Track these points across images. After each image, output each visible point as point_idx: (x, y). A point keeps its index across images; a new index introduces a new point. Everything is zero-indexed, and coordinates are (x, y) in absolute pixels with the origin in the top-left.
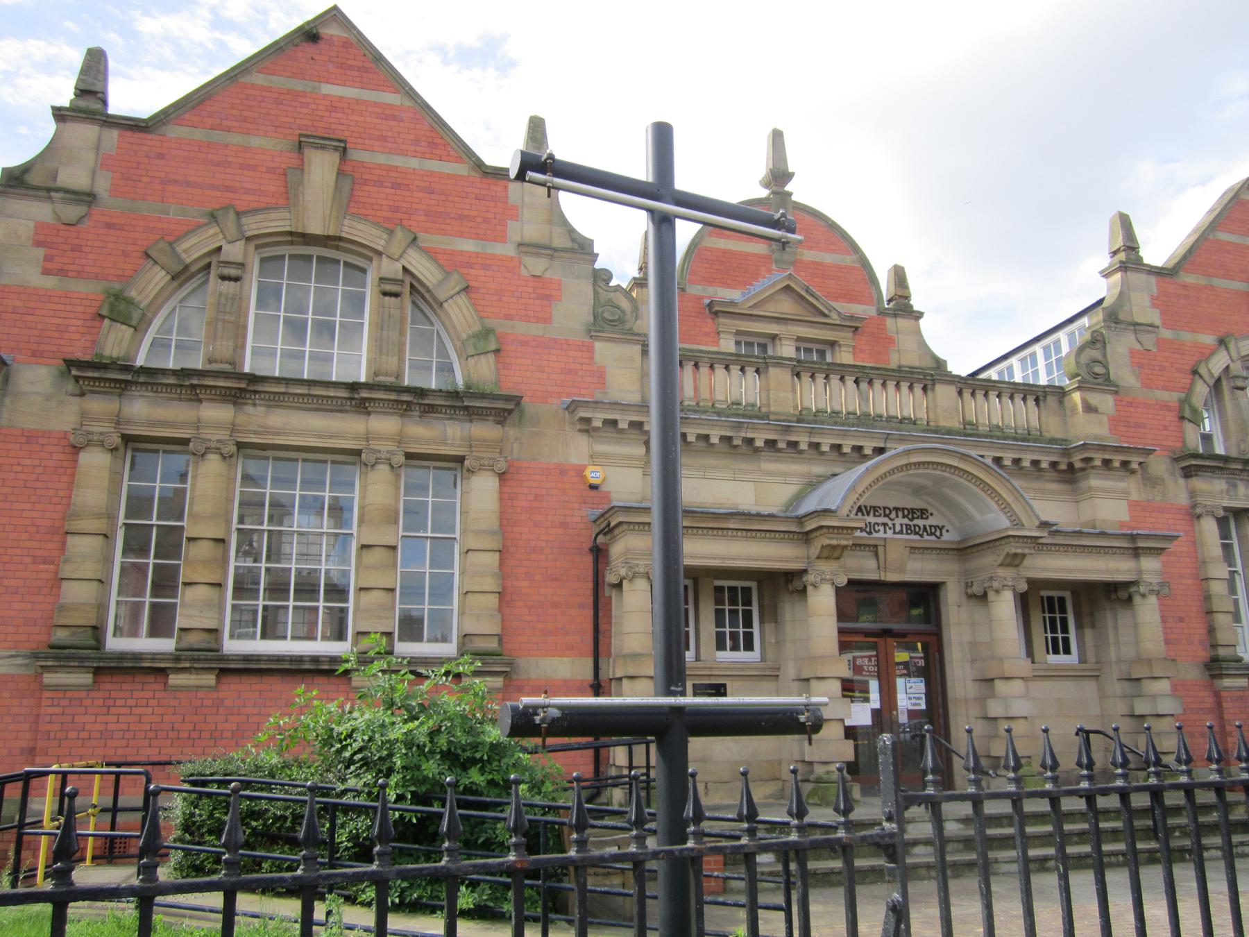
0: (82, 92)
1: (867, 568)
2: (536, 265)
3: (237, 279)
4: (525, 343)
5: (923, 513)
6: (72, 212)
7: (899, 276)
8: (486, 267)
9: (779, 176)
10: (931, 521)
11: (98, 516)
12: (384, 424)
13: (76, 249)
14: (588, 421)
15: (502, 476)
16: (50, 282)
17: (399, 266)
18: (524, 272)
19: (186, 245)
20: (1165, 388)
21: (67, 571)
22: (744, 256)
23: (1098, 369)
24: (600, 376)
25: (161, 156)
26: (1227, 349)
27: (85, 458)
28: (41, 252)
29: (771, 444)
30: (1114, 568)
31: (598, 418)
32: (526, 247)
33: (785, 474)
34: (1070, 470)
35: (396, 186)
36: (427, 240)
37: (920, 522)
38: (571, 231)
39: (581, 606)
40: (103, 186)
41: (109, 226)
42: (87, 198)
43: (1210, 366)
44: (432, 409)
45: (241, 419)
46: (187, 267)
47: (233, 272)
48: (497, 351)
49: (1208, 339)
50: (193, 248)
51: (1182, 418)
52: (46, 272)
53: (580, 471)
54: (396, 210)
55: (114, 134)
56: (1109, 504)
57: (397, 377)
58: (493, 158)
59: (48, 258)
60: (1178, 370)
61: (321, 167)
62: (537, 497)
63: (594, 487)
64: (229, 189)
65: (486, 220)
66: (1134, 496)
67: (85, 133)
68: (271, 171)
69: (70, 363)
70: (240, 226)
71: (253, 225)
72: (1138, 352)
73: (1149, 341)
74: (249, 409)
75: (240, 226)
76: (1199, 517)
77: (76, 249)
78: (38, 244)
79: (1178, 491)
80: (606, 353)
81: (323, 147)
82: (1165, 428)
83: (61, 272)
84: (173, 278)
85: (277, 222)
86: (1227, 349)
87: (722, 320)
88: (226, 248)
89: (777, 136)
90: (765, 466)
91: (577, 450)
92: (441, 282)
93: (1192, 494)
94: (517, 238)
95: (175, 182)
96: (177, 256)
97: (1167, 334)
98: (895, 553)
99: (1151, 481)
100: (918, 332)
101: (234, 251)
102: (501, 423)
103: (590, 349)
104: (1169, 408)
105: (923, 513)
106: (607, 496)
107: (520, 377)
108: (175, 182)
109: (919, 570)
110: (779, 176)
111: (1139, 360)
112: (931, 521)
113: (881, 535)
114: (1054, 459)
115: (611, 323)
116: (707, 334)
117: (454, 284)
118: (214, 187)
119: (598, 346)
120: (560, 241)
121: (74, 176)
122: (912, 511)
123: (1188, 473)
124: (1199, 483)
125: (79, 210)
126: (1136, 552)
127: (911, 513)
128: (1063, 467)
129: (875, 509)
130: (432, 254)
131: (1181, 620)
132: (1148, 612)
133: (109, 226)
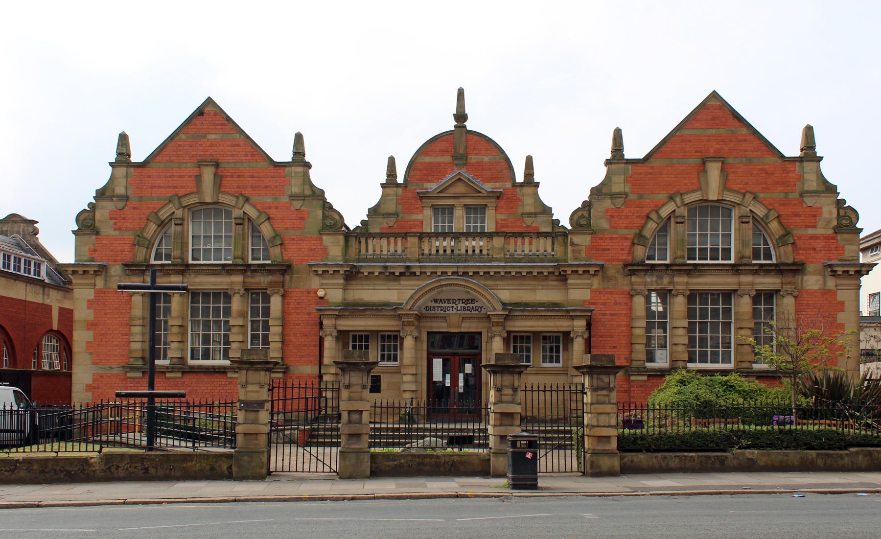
0: (119, 154)
1: (441, 327)
2: (297, 204)
3: (181, 224)
4: (293, 239)
5: (473, 301)
6: (121, 204)
7: (529, 162)
8: (277, 208)
9: (461, 117)
10: (476, 304)
11: (139, 319)
12: (238, 279)
13: (124, 219)
14: (316, 271)
15: (283, 296)
16: (117, 233)
17: (242, 212)
18: (293, 209)
19: (161, 213)
20: (626, 228)
21: (132, 338)
22: (439, 164)
23: (583, 222)
24: (325, 250)
25: (149, 177)
26: (675, 201)
27: (133, 298)
28: (113, 221)
29: (402, 274)
30: (562, 325)
31: (320, 270)
32: (293, 197)
33: (412, 286)
34: (561, 276)
35: (239, 177)
36: (253, 199)
37: (471, 305)
38: (312, 186)
39: (315, 346)
40: (130, 193)
41: (134, 208)
42: (126, 198)
43: (660, 212)
44: (255, 271)
45: (185, 280)
46: (163, 221)
47: (179, 222)
48: (281, 244)
49: (662, 196)
50: (164, 214)
51: (633, 244)
52: (115, 229)
53: (316, 292)
54: (239, 187)
55: (132, 169)
56: (579, 293)
57: (243, 259)
58: (277, 159)
59: (115, 224)
60: (637, 217)
61: (208, 174)
62: (298, 303)
63: (321, 298)
64: (175, 187)
65: (276, 187)
66: (595, 286)
67: (122, 171)
68: (190, 177)
69: (126, 265)
70: (180, 203)
71: (186, 201)
72: (612, 209)
73: (620, 202)
74: (188, 276)
75: (180, 203)
76: (632, 296)
77: (124, 219)
78: (111, 218)
79: (623, 283)
80: (327, 240)
81: (207, 165)
82: (622, 249)
83: (119, 229)
84: (159, 226)
85: (193, 199)
86: (675, 201)
87: (424, 200)
88: (176, 212)
89: (461, 93)
90: (402, 283)
91: (315, 282)
92: (258, 217)
93: (632, 284)
94: (289, 193)
95: (155, 187)
96: (158, 218)
97: (632, 197)
98: (454, 320)
99: (606, 278)
100: (536, 194)
101: (179, 213)
102: (283, 275)
103: (321, 239)
104: (626, 239)
105: (473, 301)
106: (327, 301)
107: (292, 254)
108: (155, 187)
109: (468, 327)
110: (461, 117)
111: (610, 215)
112: (476, 304)
113: (451, 312)
114: (551, 270)
115: (331, 227)
116: (418, 208)
117: (264, 217)
118: (169, 187)
119: (324, 237)
120: (308, 192)
121: (120, 190)
122: (467, 300)
123: (633, 273)
124: (634, 279)
125: (123, 203)
126: (572, 318)
127: (467, 301)
128: (557, 274)
129: (448, 300)
130: (254, 206)
131: (615, 347)
132: (578, 345)
133: (134, 208)
